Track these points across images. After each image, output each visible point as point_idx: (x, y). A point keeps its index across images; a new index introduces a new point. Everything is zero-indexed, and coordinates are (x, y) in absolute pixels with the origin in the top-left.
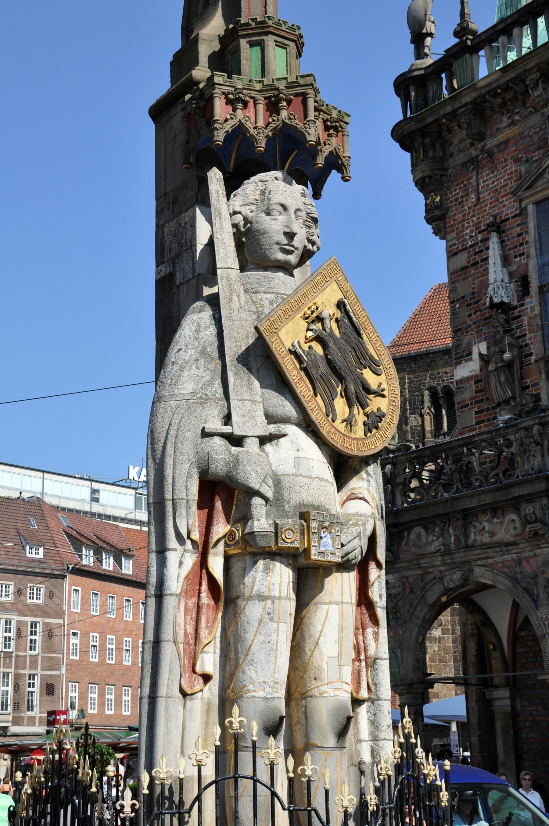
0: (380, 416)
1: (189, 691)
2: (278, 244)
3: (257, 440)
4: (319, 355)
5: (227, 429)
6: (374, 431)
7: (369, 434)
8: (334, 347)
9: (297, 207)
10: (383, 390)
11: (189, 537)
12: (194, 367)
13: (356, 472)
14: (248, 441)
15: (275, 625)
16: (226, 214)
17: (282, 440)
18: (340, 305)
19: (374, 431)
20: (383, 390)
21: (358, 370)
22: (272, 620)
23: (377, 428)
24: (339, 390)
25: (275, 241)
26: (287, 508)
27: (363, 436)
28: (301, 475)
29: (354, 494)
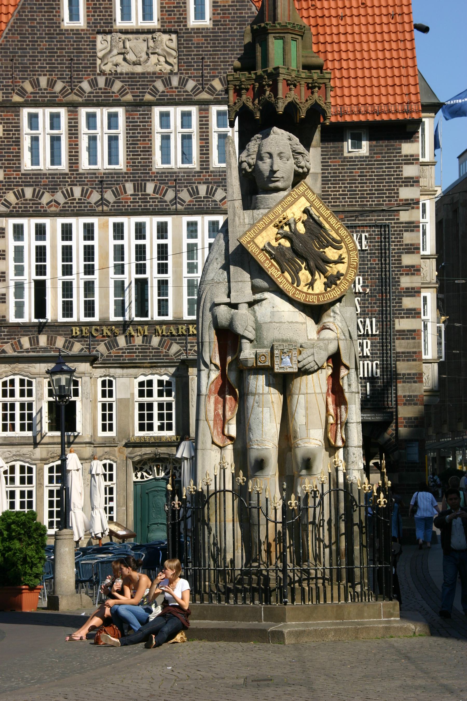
0: (339, 275)
1: (221, 445)
3: (246, 305)
4: (287, 248)
5: (227, 300)
6: (334, 286)
7: (329, 289)
10: (344, 258)
11: (211, 362)
14: (240, 306)
15: (261, 409)
17: (264, 302)
18: (306, 211)
19: (334, 286)
20: (344, 258)
22: (258, 406)
24: (303, 266)
26: (266, 342)
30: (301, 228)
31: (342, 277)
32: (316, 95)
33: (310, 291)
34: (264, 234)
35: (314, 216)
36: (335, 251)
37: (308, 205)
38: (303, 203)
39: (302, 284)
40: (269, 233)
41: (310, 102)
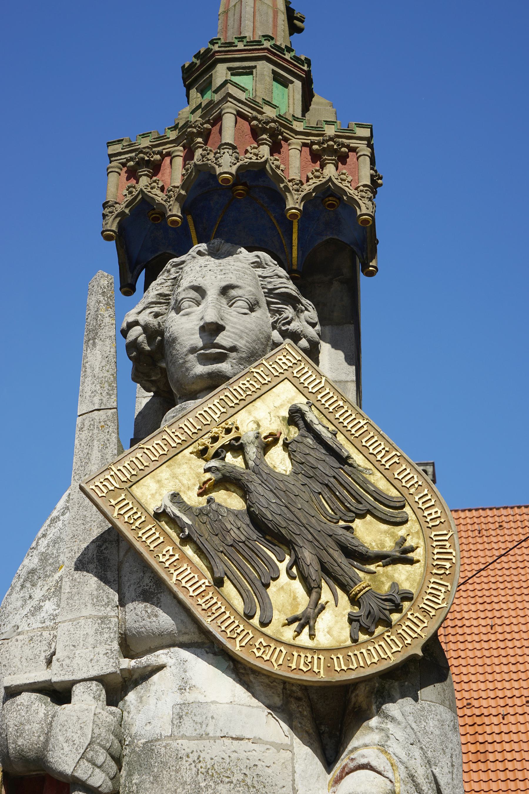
0: (398, 600)
2: (193, 350)
5: (41, 675)
6: (380, 630)
7: (363, 637)
8: (260, 489)
9: (224, 284)
10: (412, 549)
12: (28, 585)
13: (361, 716)
14: (78, 690)
16: (109, 331)
17: (155, 678)
18: (295, 417)
20: (412, 549)
21: (341, 523)
23: (388, 624)
25: (188, 347)
27: (349, 643)
28: (183, 737)
29: (352, 760)
30: (279, 460)
31: (406, 605)
32: (330, 171)
33: (304, 639)
34: (164, 473)
35: (319, 428)
36: (385, 527)
37: (301, 401)
38: (285, 396)
39: (278, 618)
40: (178, 471)
41: (314, 182)
